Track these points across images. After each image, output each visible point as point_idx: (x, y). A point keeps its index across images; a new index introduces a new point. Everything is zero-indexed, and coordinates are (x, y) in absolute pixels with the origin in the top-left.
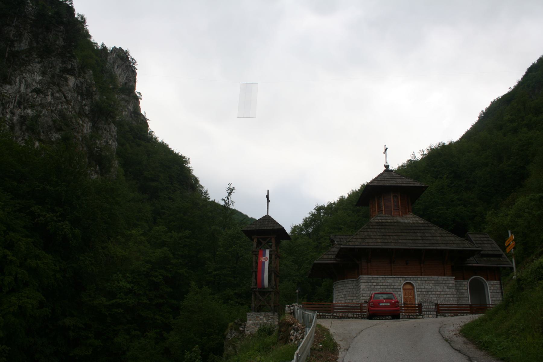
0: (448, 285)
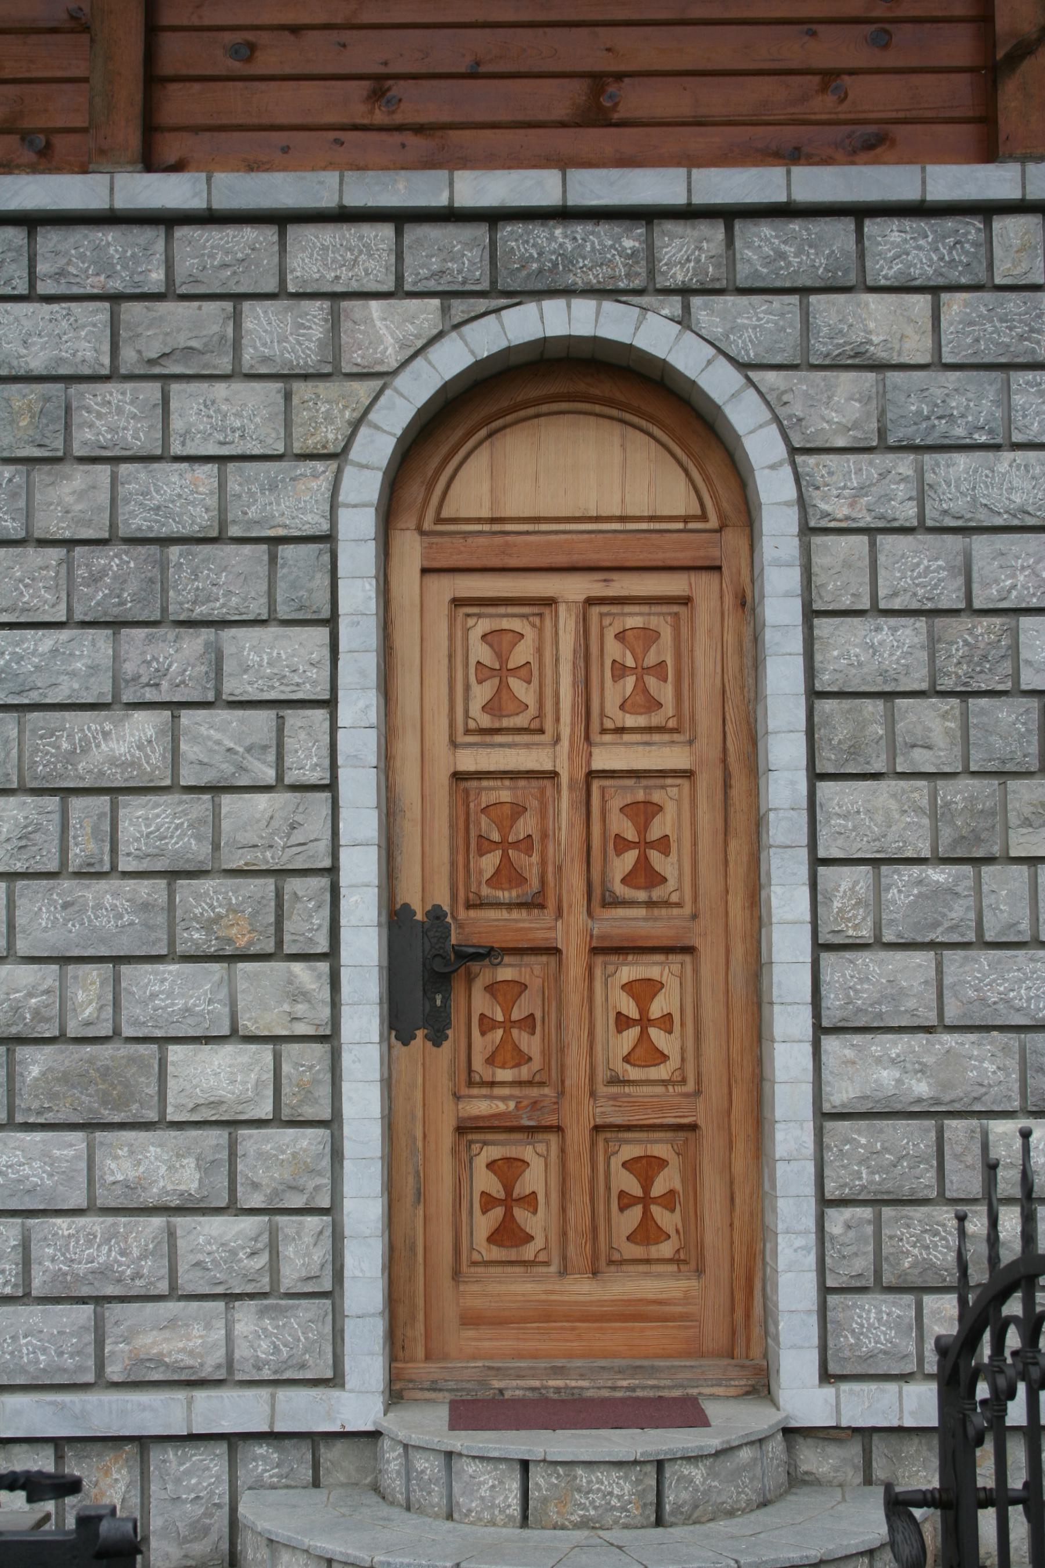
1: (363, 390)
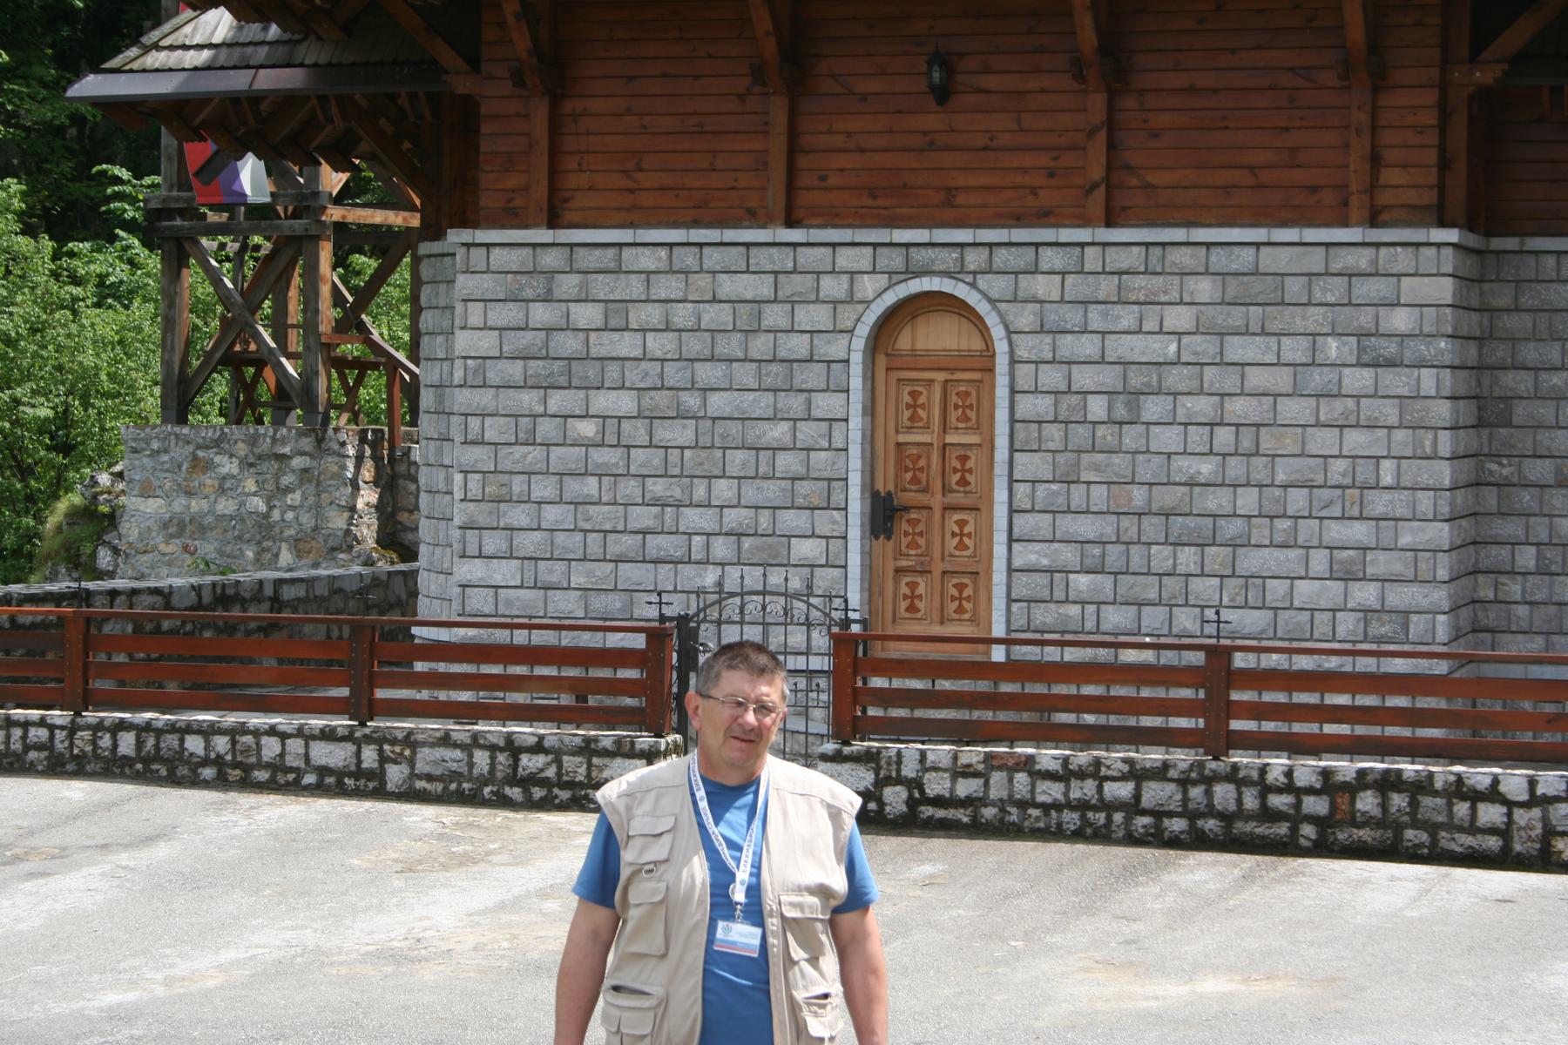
0: (1365, 318)
1: (861, 308)
